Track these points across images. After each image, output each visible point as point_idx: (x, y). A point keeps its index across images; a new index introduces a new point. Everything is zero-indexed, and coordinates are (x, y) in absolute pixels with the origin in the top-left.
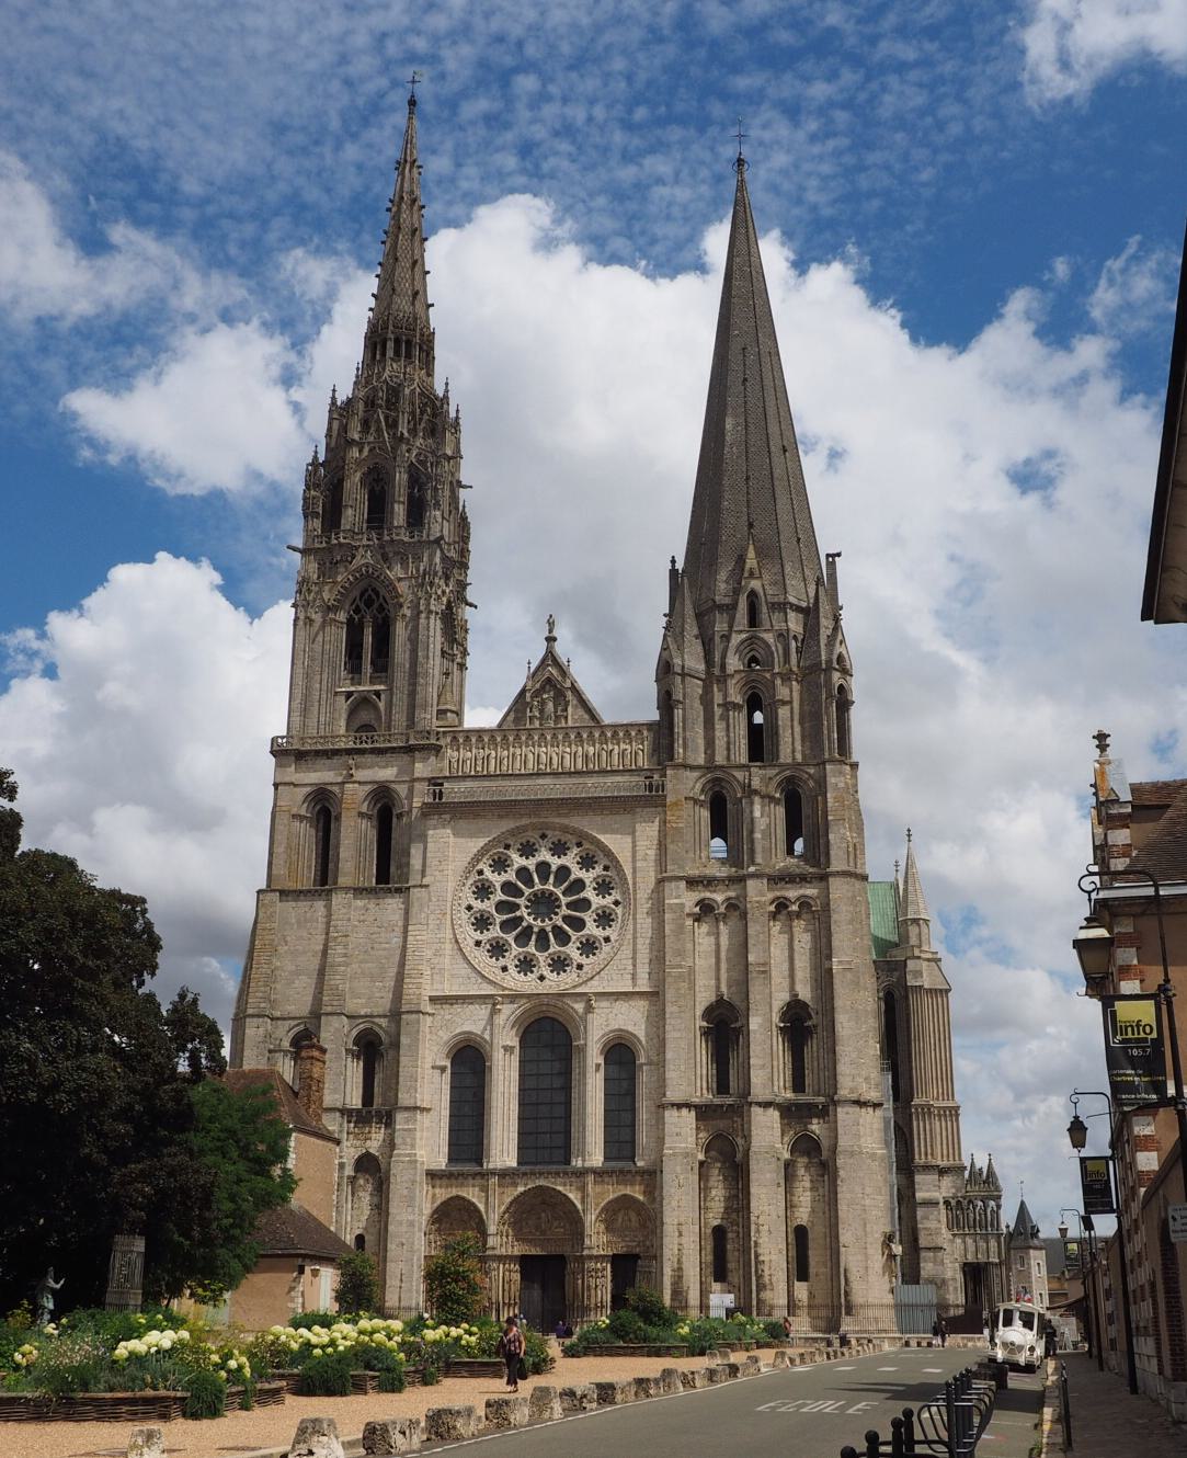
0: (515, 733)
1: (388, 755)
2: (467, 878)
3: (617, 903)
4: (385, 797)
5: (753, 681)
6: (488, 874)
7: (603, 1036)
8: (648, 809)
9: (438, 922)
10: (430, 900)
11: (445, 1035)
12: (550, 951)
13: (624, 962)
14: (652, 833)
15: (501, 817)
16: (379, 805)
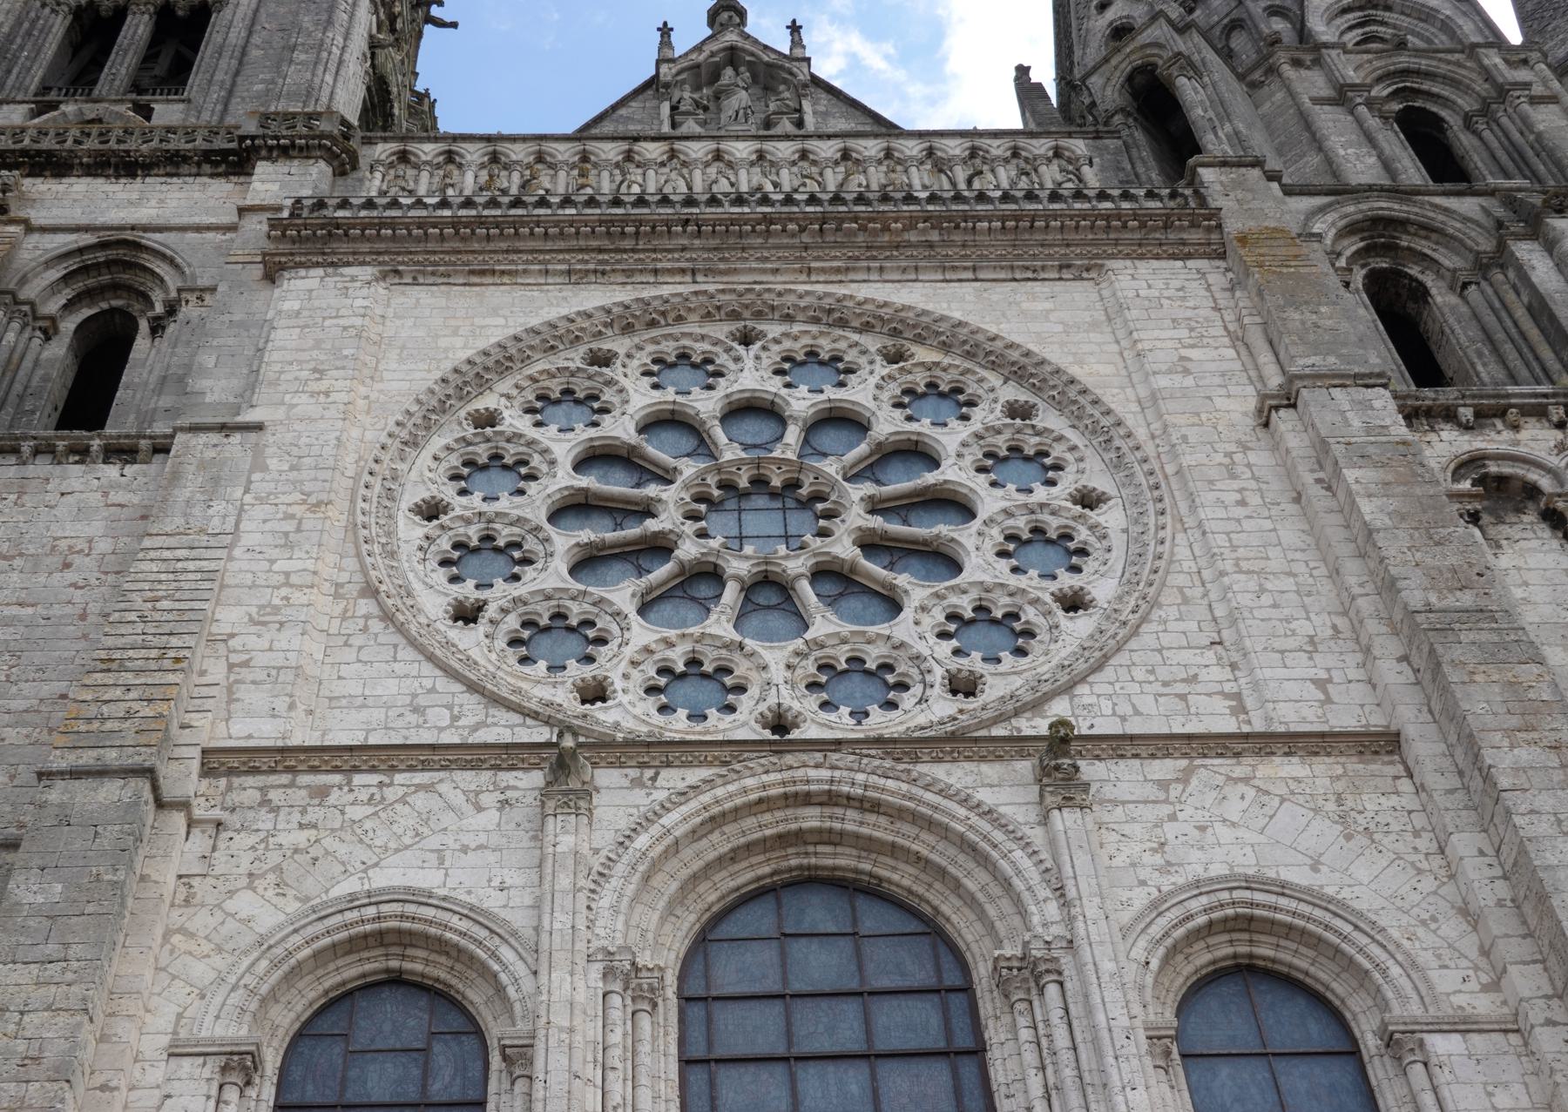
0: (624, 146)
1: (148, 180)
2: (428, 425)
3: (1088, 500)
4: (115, 288)
5: (1405, 73)
6: (515, 421)
7: (1156, 907)
8: (1155, 264)
9: (289, 526)
10: (259, 465)
11: (263, 912)
12: (809, 635)
13: (1186, 656)
14: (1189, 313)
15: (574, 277)
16: (87, 312)
